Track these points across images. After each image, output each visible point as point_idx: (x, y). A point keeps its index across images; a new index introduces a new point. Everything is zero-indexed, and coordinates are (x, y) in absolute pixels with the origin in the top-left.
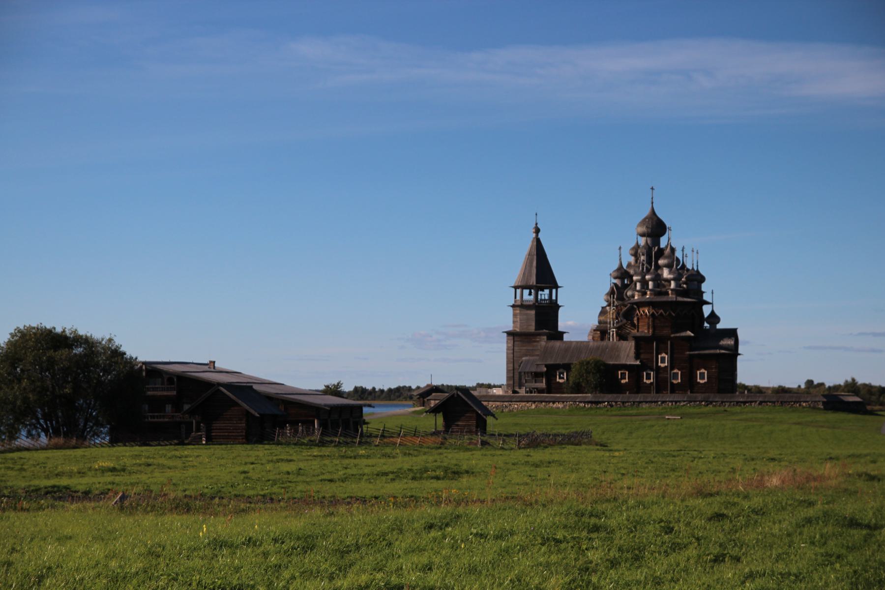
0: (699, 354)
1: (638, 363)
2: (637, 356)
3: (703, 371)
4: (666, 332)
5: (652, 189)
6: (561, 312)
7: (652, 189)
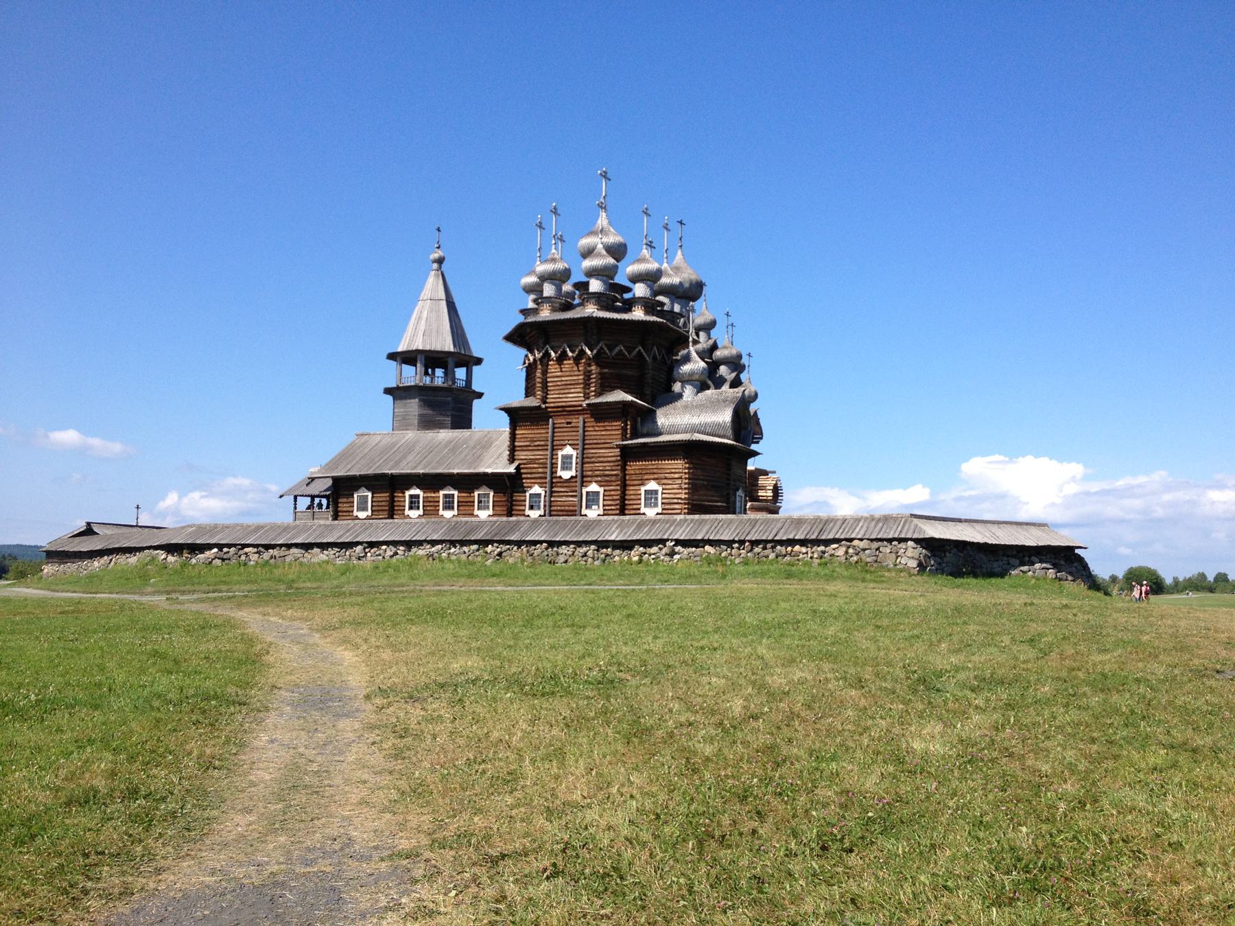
0: (645, 444)
1: (511, 469)
2: (512, 459)
3: (652, 485)
4: (574, 397)
5: (681, 223)
6: (476, 404)
7: (681, 223)
